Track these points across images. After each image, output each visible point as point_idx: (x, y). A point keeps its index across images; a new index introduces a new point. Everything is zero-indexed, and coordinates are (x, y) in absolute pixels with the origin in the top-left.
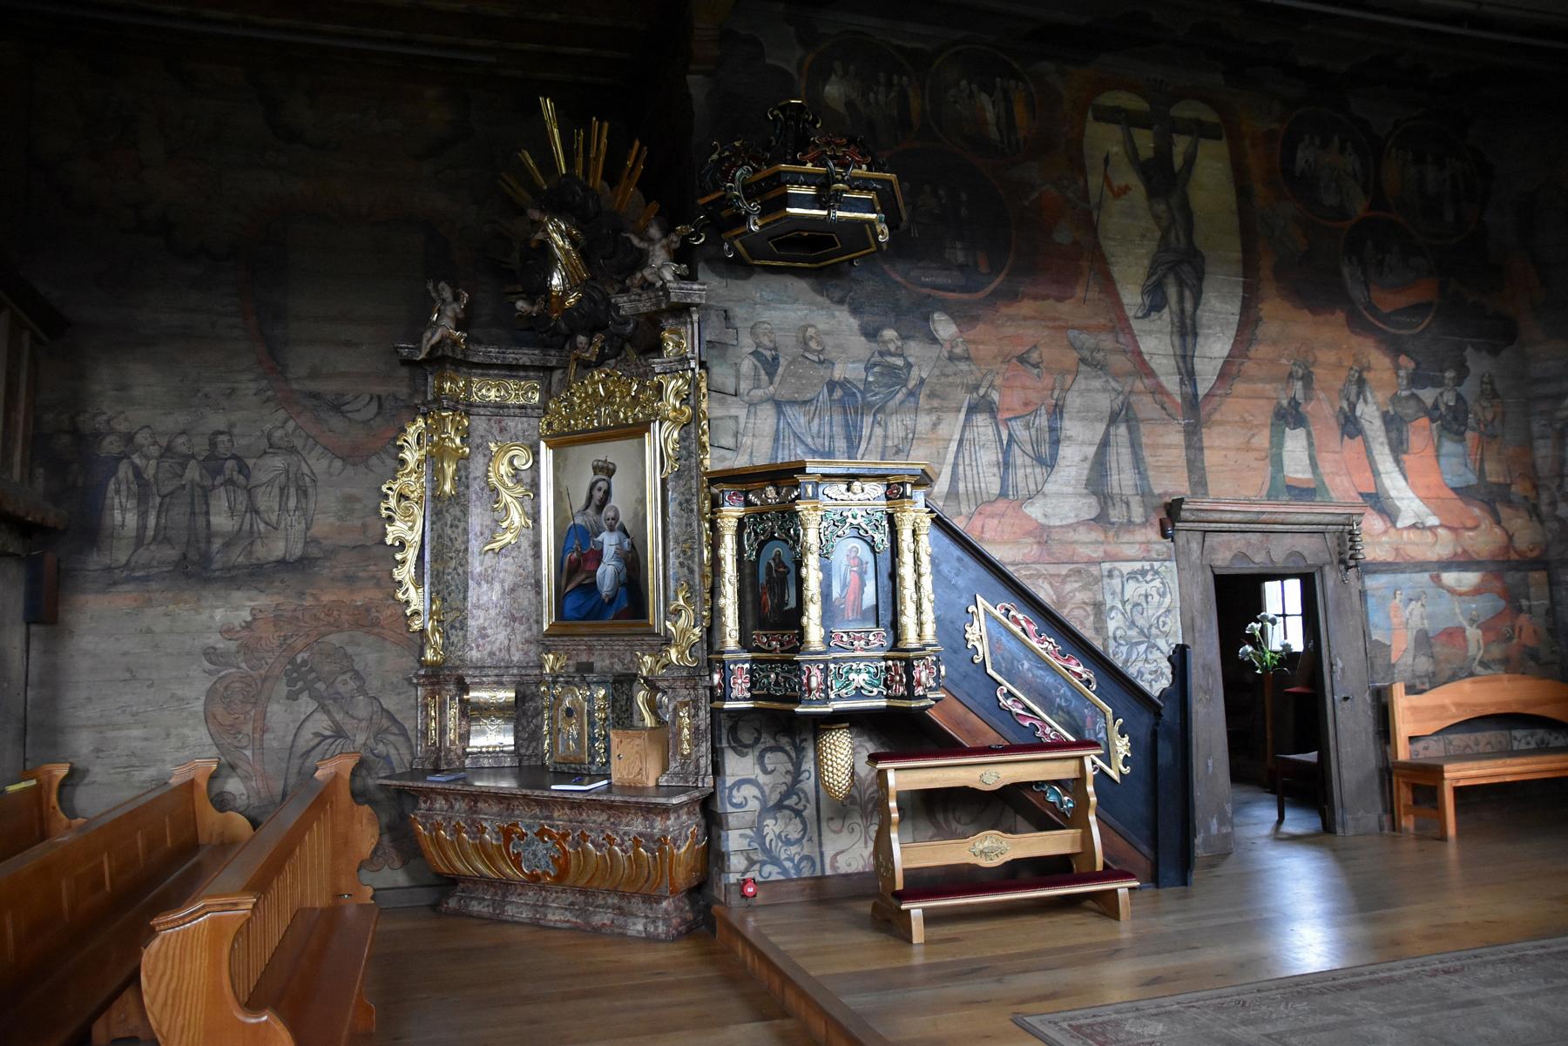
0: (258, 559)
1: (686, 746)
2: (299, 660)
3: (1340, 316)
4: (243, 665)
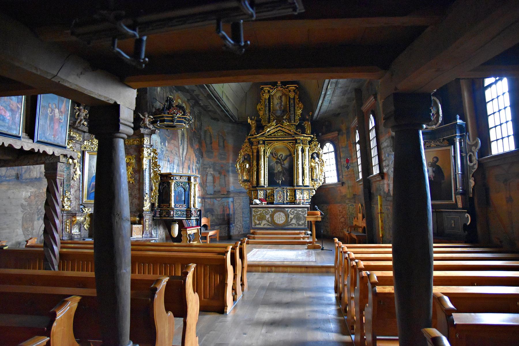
0: (31, 177)
1: (147, 228)
2: (39, 208)
3: (193, 149)
4: (29, 209)
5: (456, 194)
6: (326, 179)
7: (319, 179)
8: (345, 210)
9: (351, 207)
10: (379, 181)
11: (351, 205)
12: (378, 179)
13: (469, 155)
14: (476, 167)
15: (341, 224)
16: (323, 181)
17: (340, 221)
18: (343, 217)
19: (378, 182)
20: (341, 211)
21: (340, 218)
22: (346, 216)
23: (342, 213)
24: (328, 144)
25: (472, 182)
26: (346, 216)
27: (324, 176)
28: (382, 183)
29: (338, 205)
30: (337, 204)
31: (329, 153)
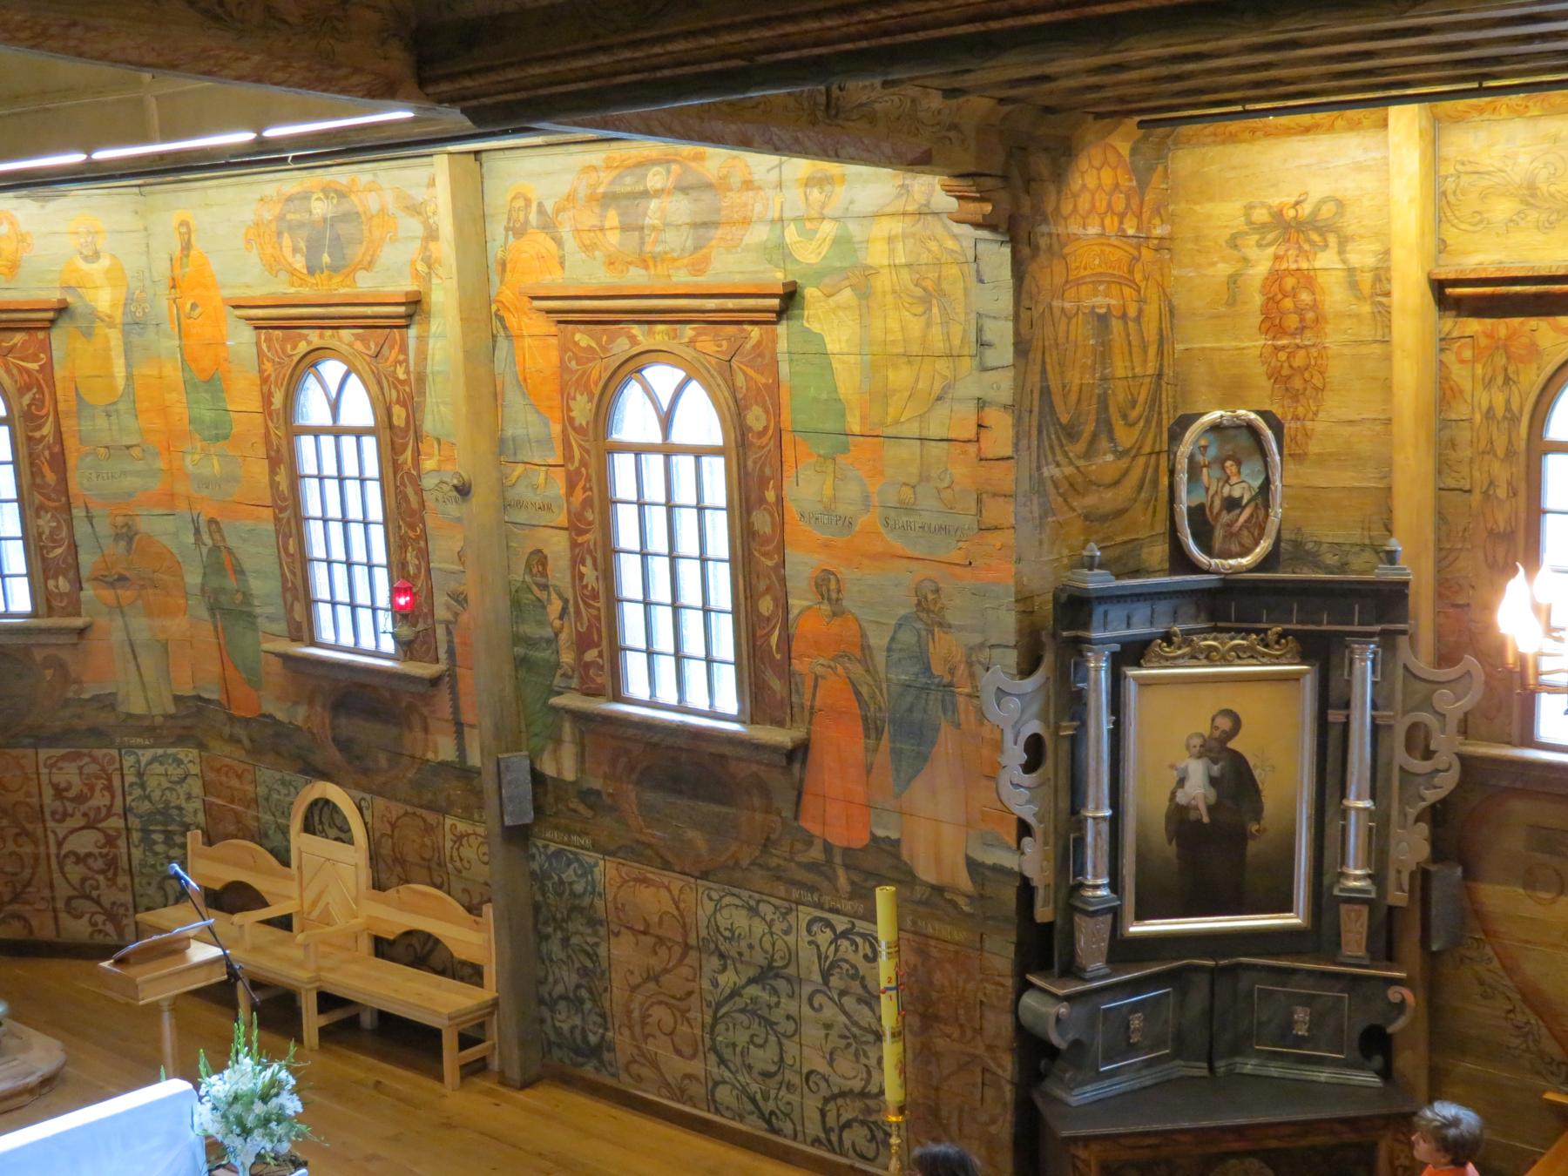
8: (109, 788)
9: (158, 768)
11: (154, 759)
17: (66, 848)
20: (72, 794)
21: (61, 833)
22: (115, 823)
23: (81, 799)
26: (115, 823)
29: (44, 753)
30: (36, 747)
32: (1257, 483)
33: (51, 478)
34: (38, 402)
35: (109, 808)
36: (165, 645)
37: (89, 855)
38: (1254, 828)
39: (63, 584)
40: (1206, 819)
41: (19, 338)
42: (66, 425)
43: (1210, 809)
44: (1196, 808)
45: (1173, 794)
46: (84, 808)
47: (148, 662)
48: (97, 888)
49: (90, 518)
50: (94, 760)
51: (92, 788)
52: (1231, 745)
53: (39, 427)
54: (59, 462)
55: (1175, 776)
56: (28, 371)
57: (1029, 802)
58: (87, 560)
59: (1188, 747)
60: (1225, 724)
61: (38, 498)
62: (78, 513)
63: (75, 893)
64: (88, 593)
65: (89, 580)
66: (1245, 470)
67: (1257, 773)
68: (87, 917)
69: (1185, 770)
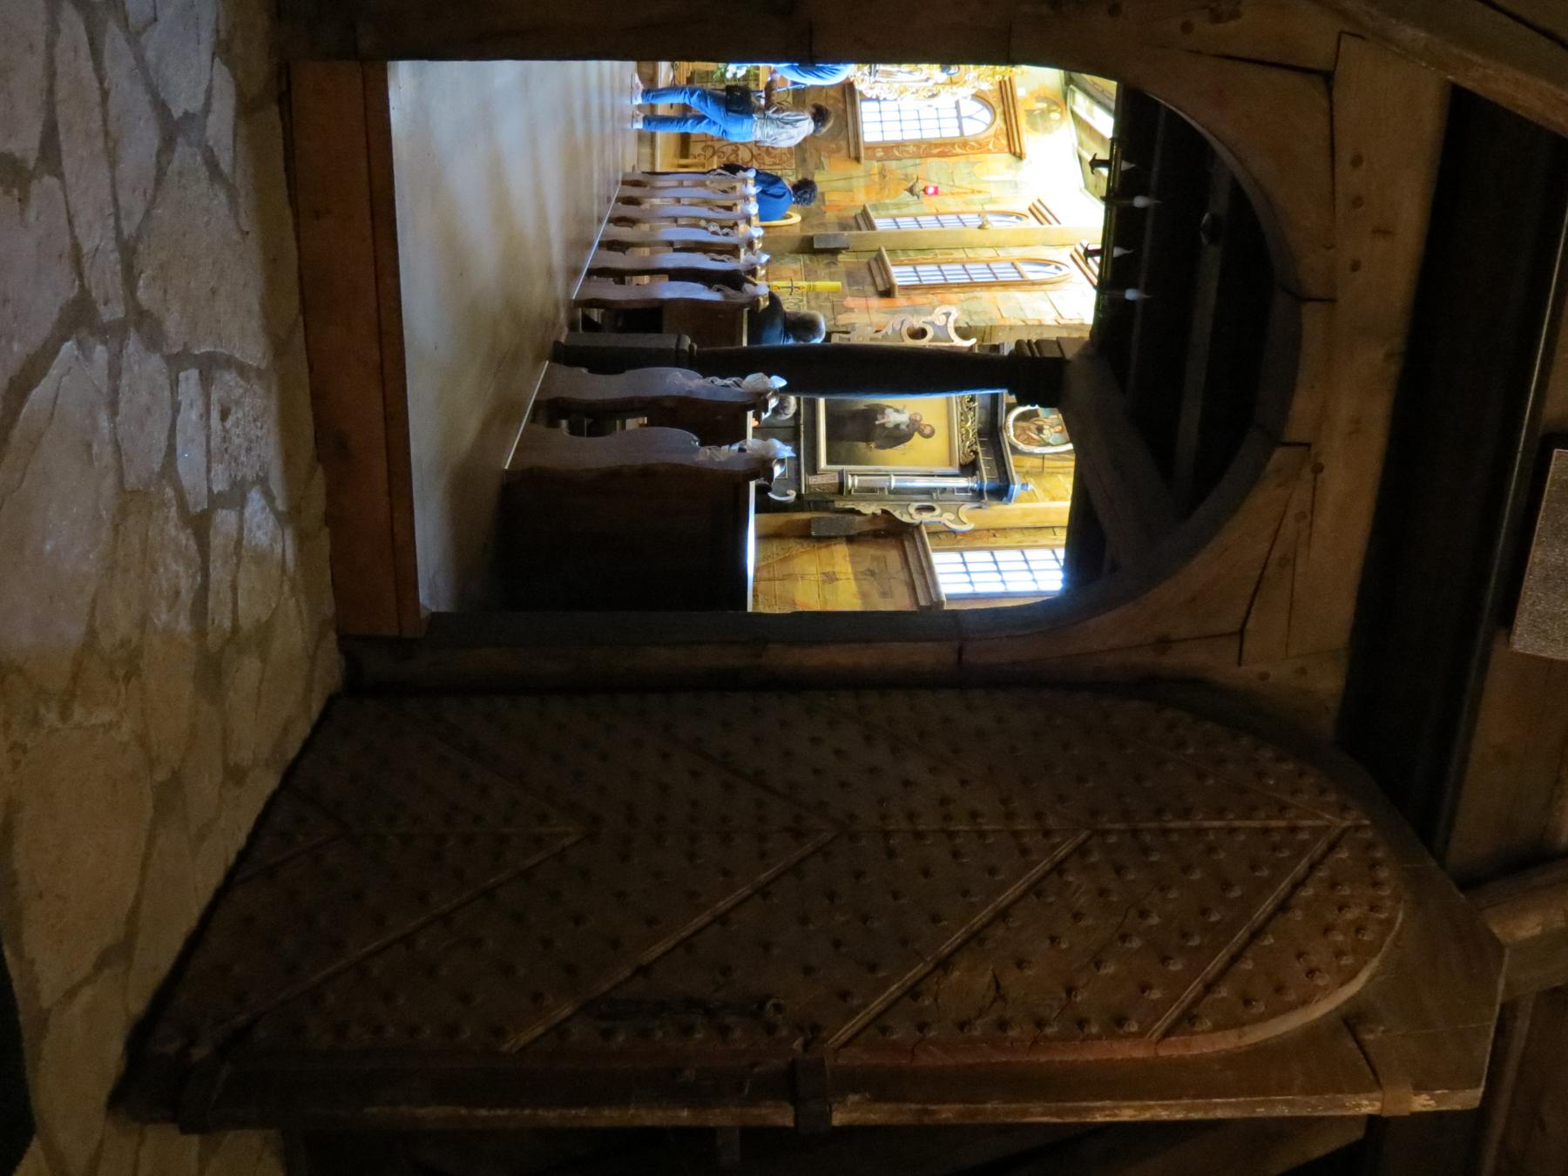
5: (841, 474)
6: (876, 104)
7: (876, 82)
8: (775, 164)
10: (874, 283)
12: (879, 280)
13: (934, 505)
14: (906, 519)
15: (730, 147)
16: (869, 94)
18: (753, 156)
19: (869, 279)
24: (986, 115)
25: (869, 509)
27: (885, 99)
28: (870, 289)
31: (959, 117)
32: (1051, 441)
33: (935, 151)
34: (973, 148)
35: (764, 164)
36: (851, 191)
37: (737, 155)
38: (873, 445)
39: (880, 154)
40: (877, 422)
41: (1004, 142)
42: (963, 158)
43: (883, 425)
44: (883, 418)
45: (891, 407)
46: (764, 154)
47: (841, 184)
48: (719, 157)
49: (915, 165)
50: (788, 159)
51: (775, 157)
52: (916, 434)
53: (959, 147)
54: (942, 155)
55: (900, 408)
56: (988, 145)
57: (894, 329)
58: (893, 164)
59: (915, 414)
60: (927, 431)
61: (924, 146)
62: (918, 161)
63: (716, 148)
64: (876, 164)
65: (883, 166)
66: (1057, 435)
67: (902, 446)
68: (700, 152)
69: (903, 413)
